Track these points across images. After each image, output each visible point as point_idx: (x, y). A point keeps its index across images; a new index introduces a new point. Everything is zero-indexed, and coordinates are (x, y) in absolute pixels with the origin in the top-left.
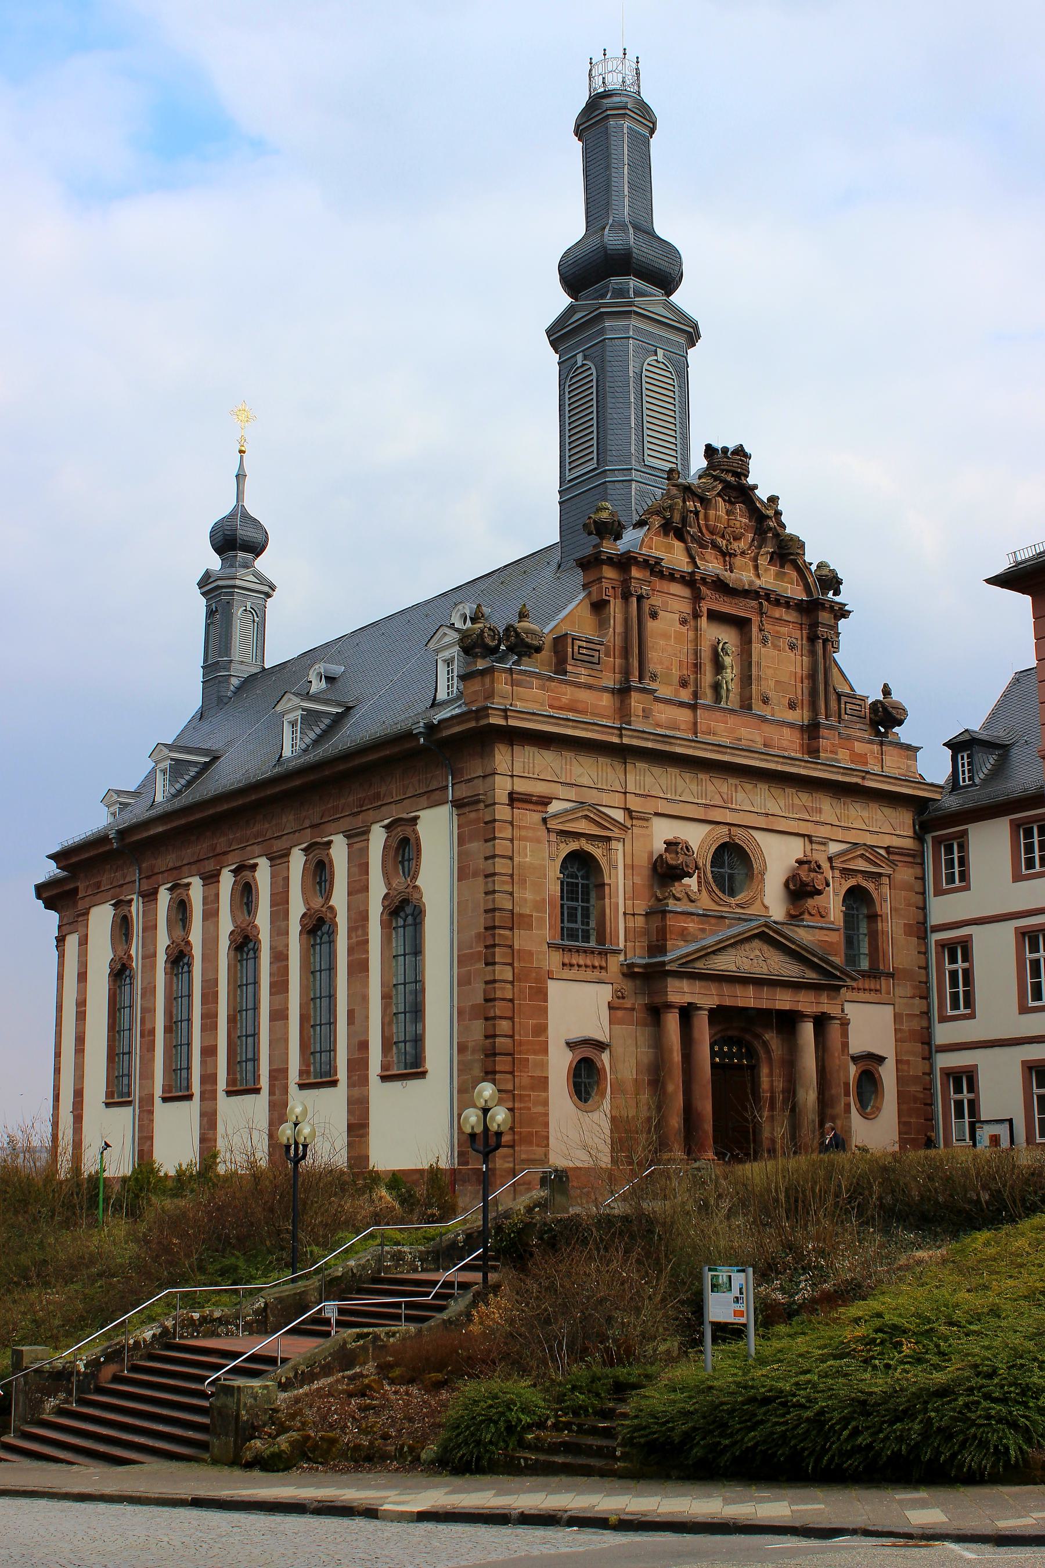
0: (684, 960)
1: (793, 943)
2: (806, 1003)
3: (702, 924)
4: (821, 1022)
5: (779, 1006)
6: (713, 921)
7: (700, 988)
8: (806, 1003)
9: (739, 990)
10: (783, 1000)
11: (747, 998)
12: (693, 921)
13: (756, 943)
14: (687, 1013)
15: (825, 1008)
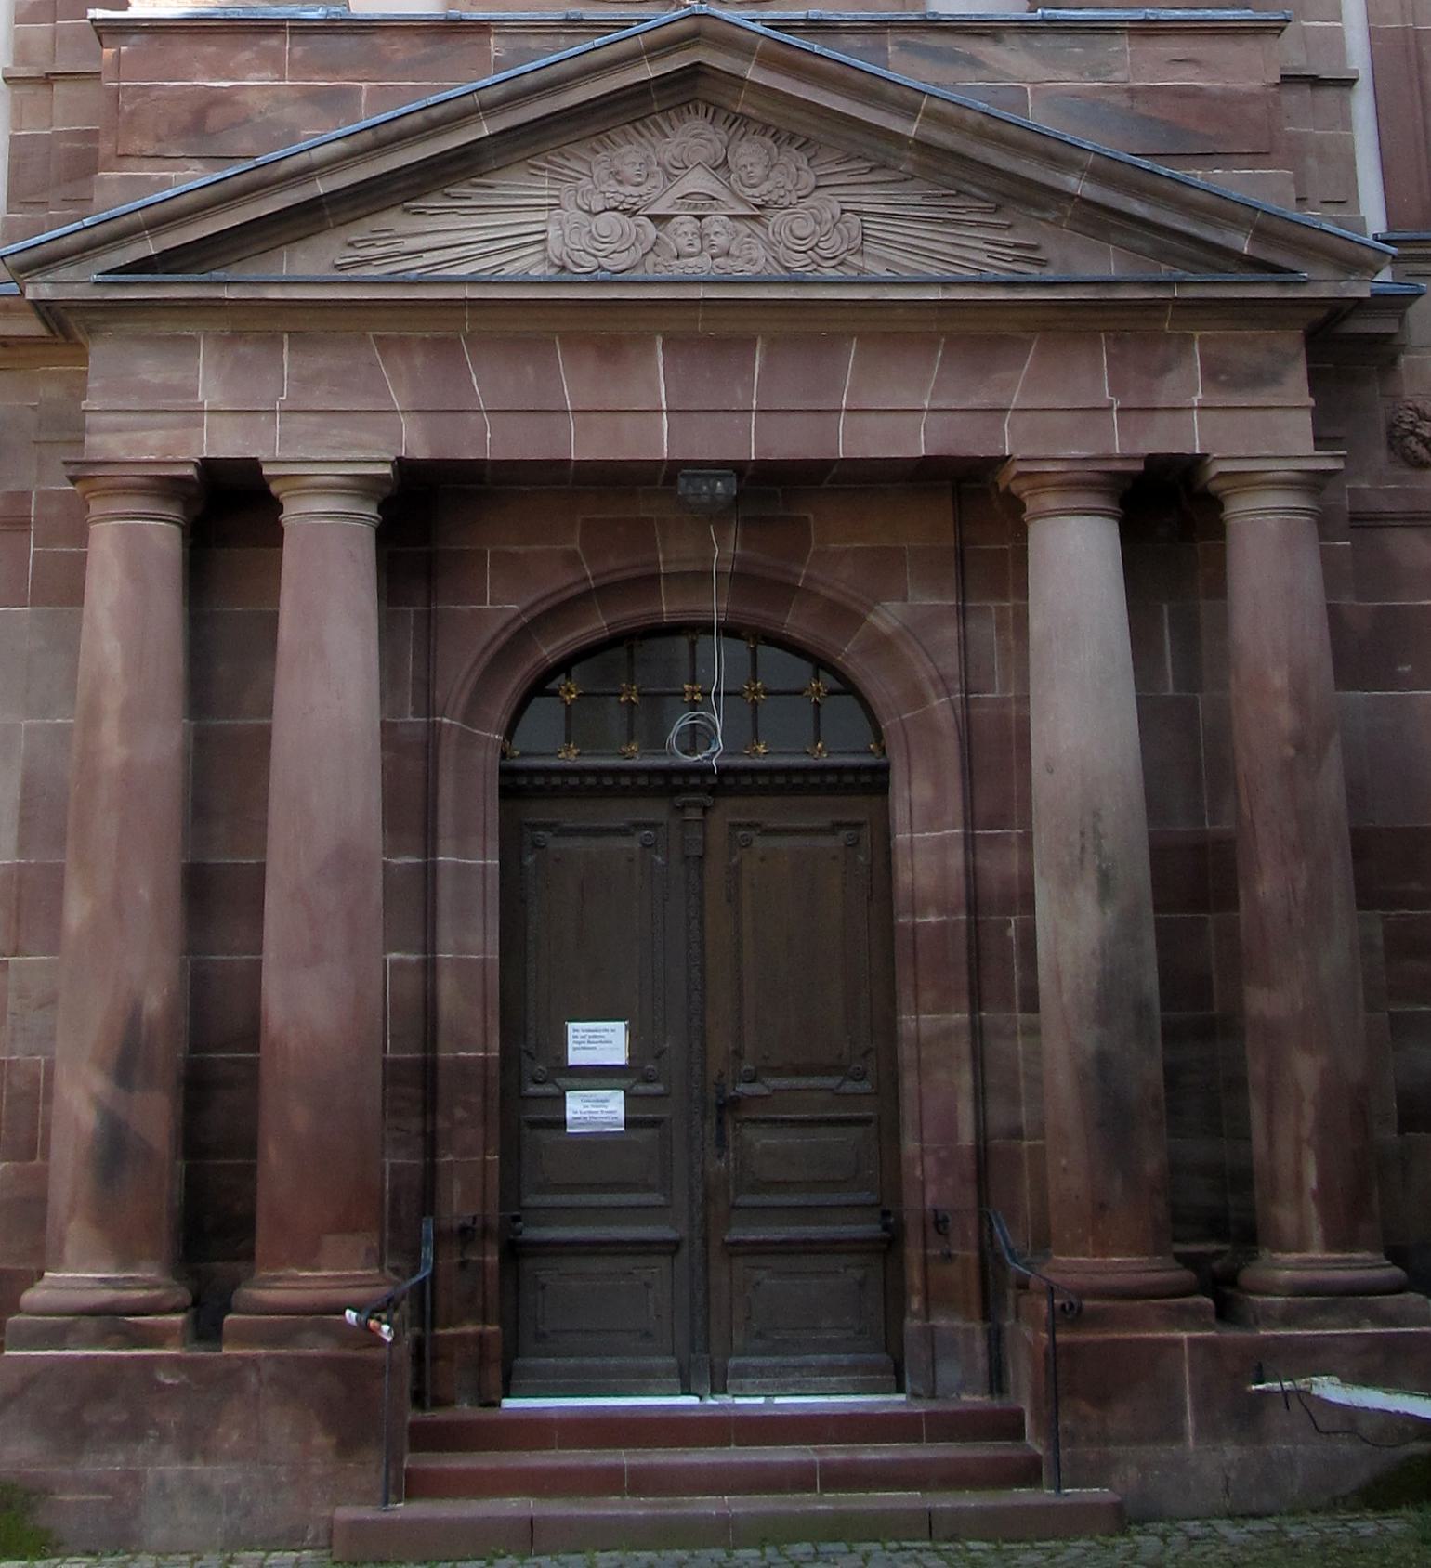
0: (150, 247)
1: (910, 111)
2: (1048, 416)
3: (333, 70)
4: (1166, 513)
5: (851, 440)
6: (399, 49)
7: (304, 383)
8: (1048, 416)
9: (572, 383)
10: (895, 414)
11: (644, 415)
12: (275, 61)
13: (692, 137)
14: (226, 512)
15: (1192, 437)
